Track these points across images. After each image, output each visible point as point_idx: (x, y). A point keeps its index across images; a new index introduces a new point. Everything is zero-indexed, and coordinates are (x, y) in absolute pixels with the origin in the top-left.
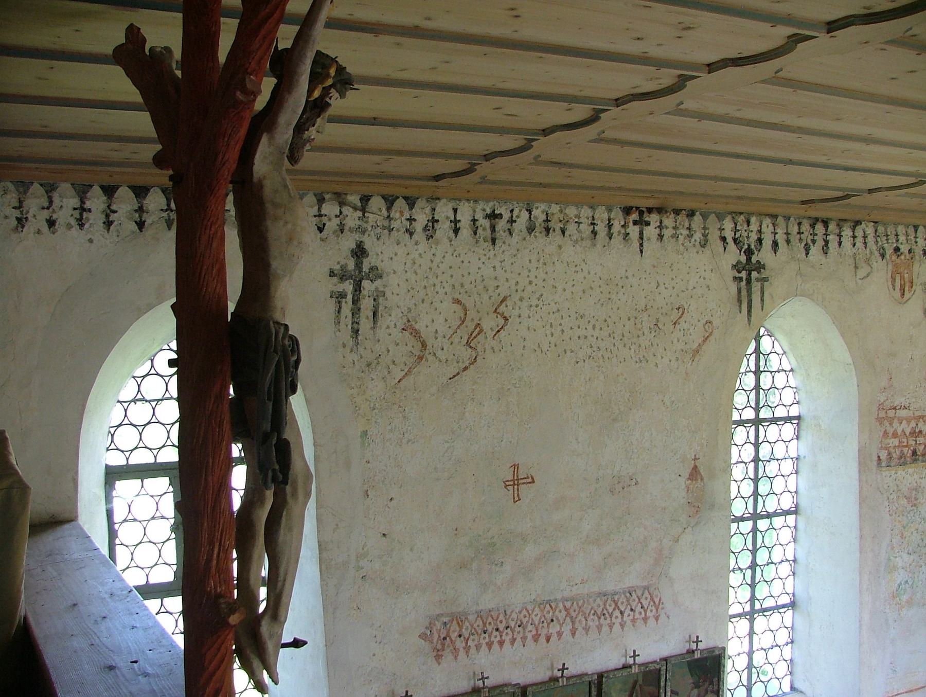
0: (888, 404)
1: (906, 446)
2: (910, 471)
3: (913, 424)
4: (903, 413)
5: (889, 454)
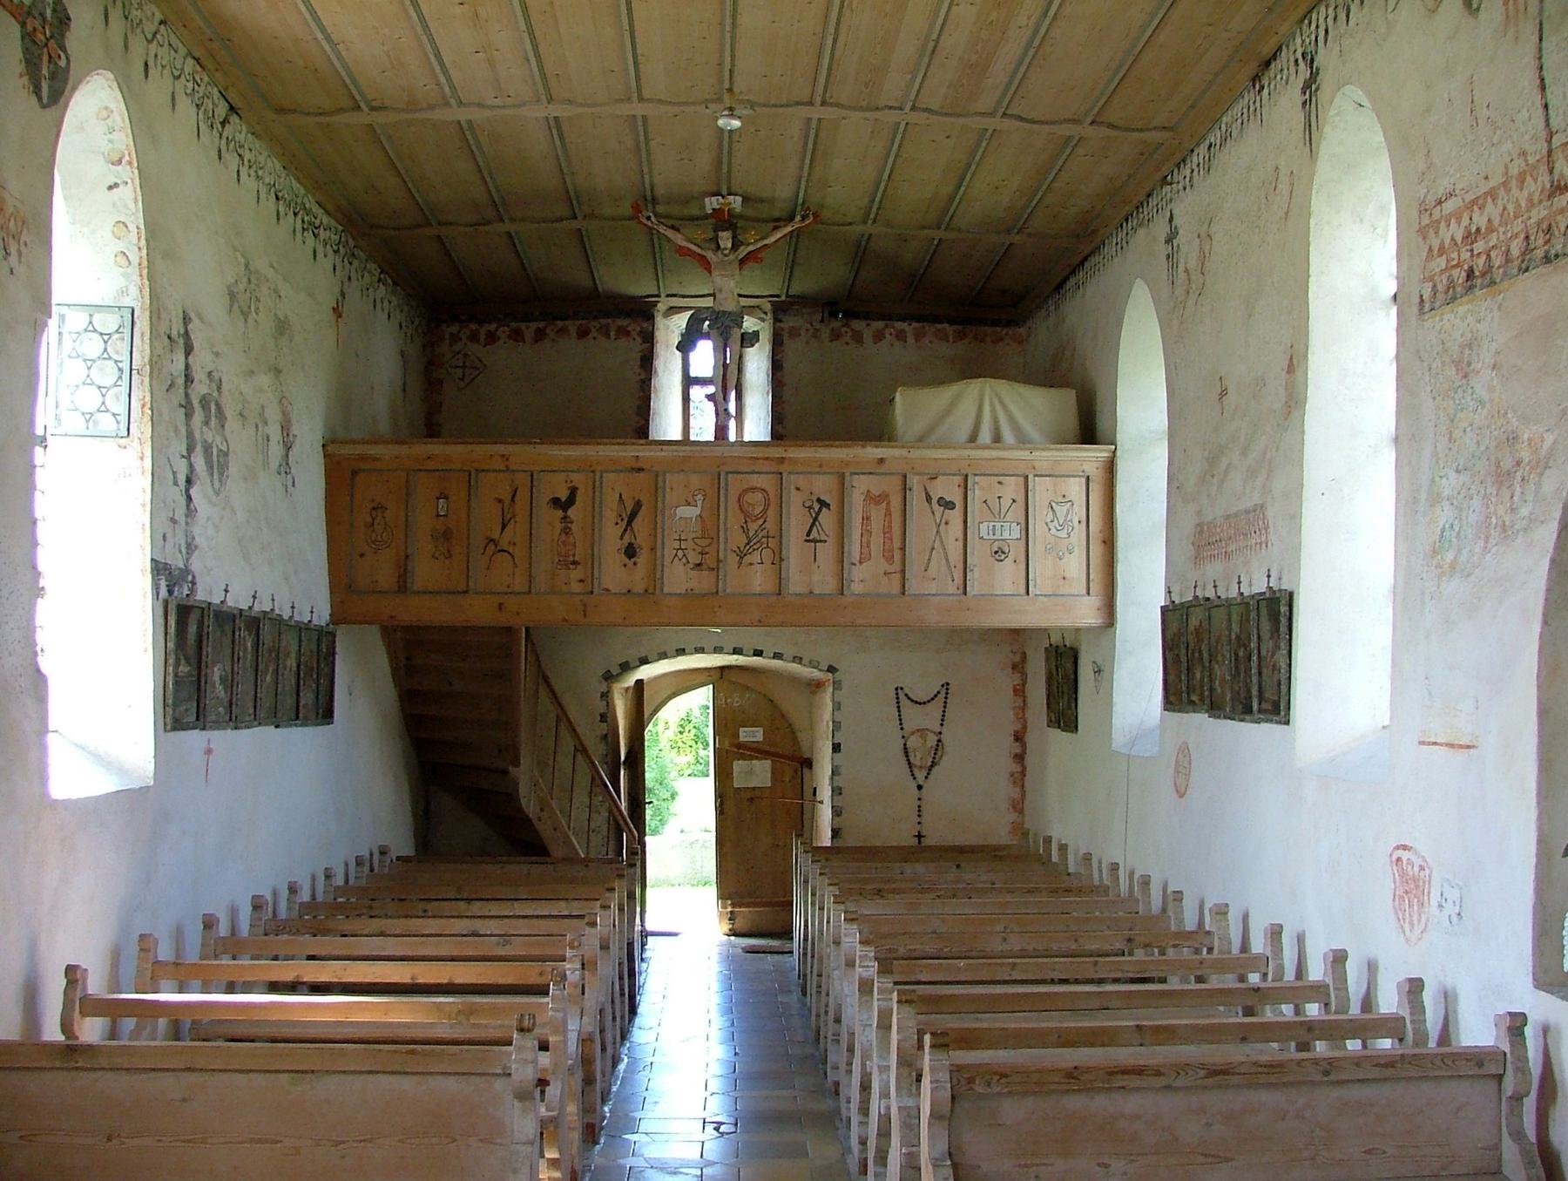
0: (1431, 199)
1: (1457, 266)
2: (1461, 310)
3: (1465, 221)
4: (1449, 206)
5: (1434, 286)
